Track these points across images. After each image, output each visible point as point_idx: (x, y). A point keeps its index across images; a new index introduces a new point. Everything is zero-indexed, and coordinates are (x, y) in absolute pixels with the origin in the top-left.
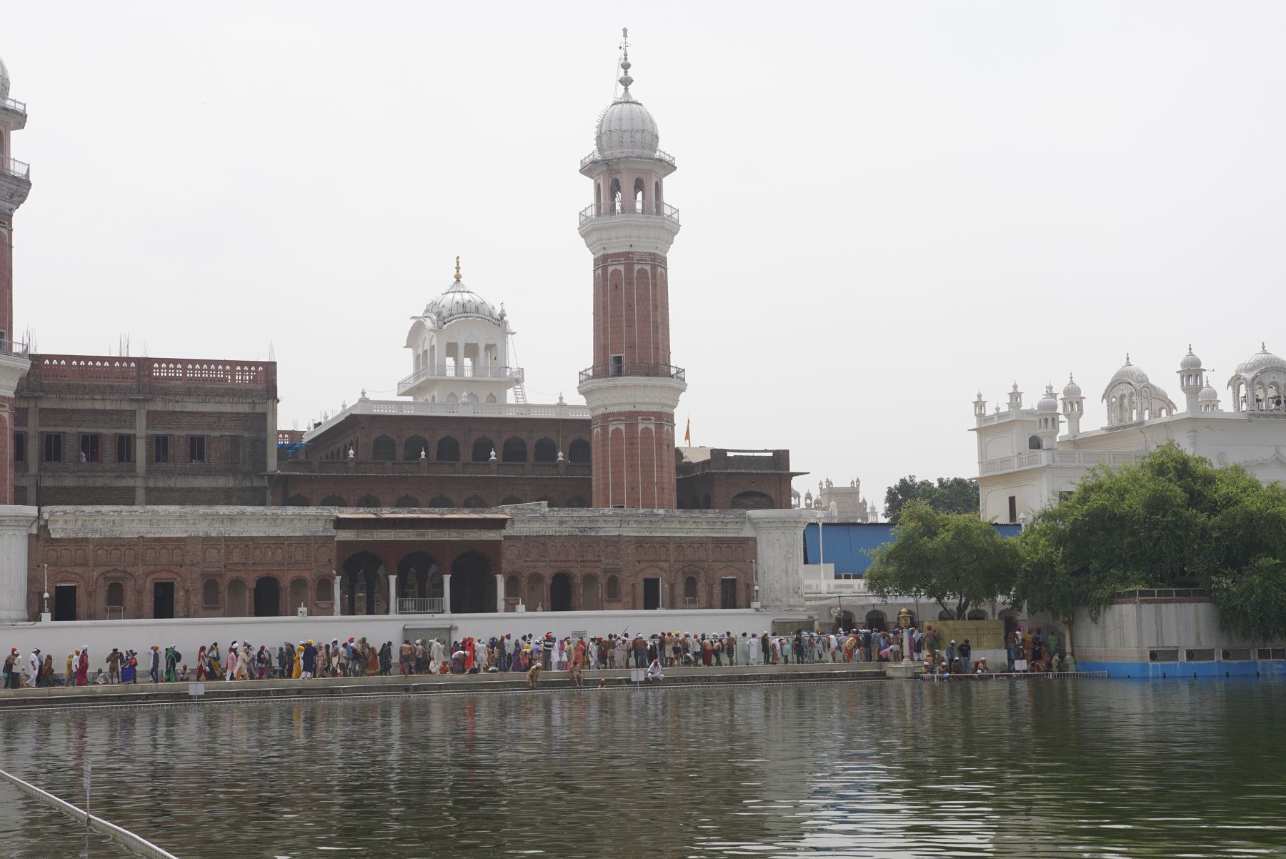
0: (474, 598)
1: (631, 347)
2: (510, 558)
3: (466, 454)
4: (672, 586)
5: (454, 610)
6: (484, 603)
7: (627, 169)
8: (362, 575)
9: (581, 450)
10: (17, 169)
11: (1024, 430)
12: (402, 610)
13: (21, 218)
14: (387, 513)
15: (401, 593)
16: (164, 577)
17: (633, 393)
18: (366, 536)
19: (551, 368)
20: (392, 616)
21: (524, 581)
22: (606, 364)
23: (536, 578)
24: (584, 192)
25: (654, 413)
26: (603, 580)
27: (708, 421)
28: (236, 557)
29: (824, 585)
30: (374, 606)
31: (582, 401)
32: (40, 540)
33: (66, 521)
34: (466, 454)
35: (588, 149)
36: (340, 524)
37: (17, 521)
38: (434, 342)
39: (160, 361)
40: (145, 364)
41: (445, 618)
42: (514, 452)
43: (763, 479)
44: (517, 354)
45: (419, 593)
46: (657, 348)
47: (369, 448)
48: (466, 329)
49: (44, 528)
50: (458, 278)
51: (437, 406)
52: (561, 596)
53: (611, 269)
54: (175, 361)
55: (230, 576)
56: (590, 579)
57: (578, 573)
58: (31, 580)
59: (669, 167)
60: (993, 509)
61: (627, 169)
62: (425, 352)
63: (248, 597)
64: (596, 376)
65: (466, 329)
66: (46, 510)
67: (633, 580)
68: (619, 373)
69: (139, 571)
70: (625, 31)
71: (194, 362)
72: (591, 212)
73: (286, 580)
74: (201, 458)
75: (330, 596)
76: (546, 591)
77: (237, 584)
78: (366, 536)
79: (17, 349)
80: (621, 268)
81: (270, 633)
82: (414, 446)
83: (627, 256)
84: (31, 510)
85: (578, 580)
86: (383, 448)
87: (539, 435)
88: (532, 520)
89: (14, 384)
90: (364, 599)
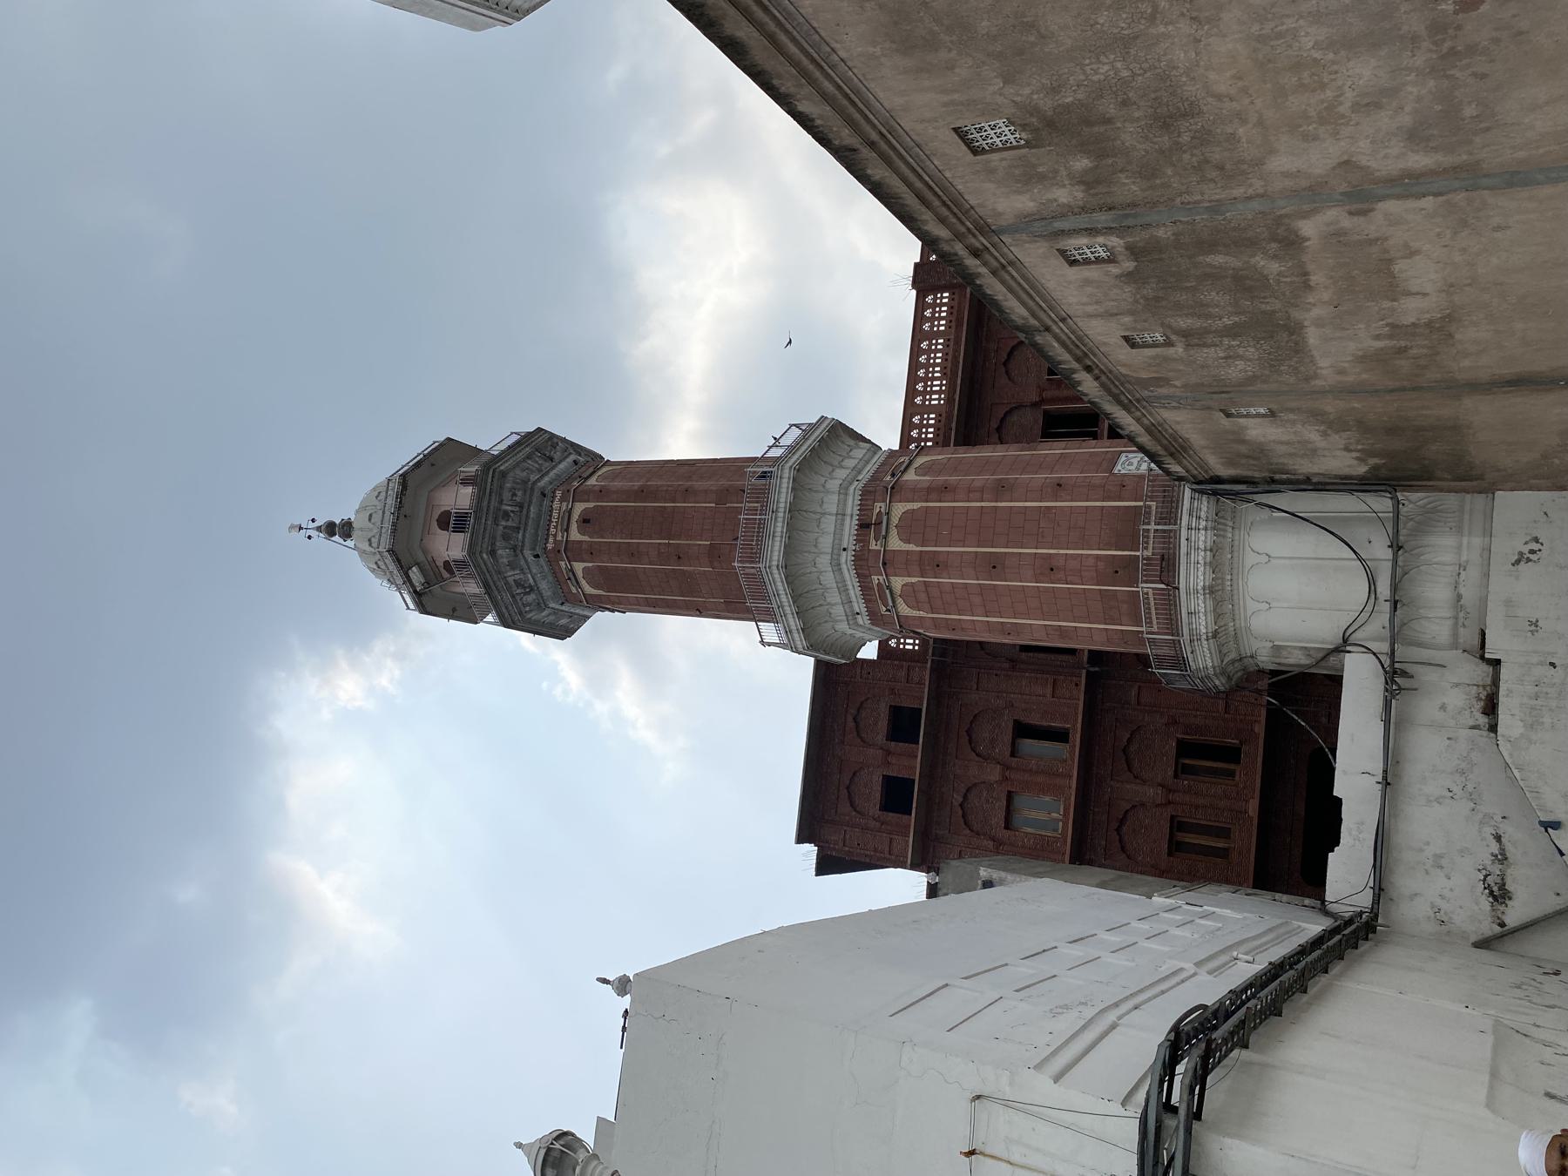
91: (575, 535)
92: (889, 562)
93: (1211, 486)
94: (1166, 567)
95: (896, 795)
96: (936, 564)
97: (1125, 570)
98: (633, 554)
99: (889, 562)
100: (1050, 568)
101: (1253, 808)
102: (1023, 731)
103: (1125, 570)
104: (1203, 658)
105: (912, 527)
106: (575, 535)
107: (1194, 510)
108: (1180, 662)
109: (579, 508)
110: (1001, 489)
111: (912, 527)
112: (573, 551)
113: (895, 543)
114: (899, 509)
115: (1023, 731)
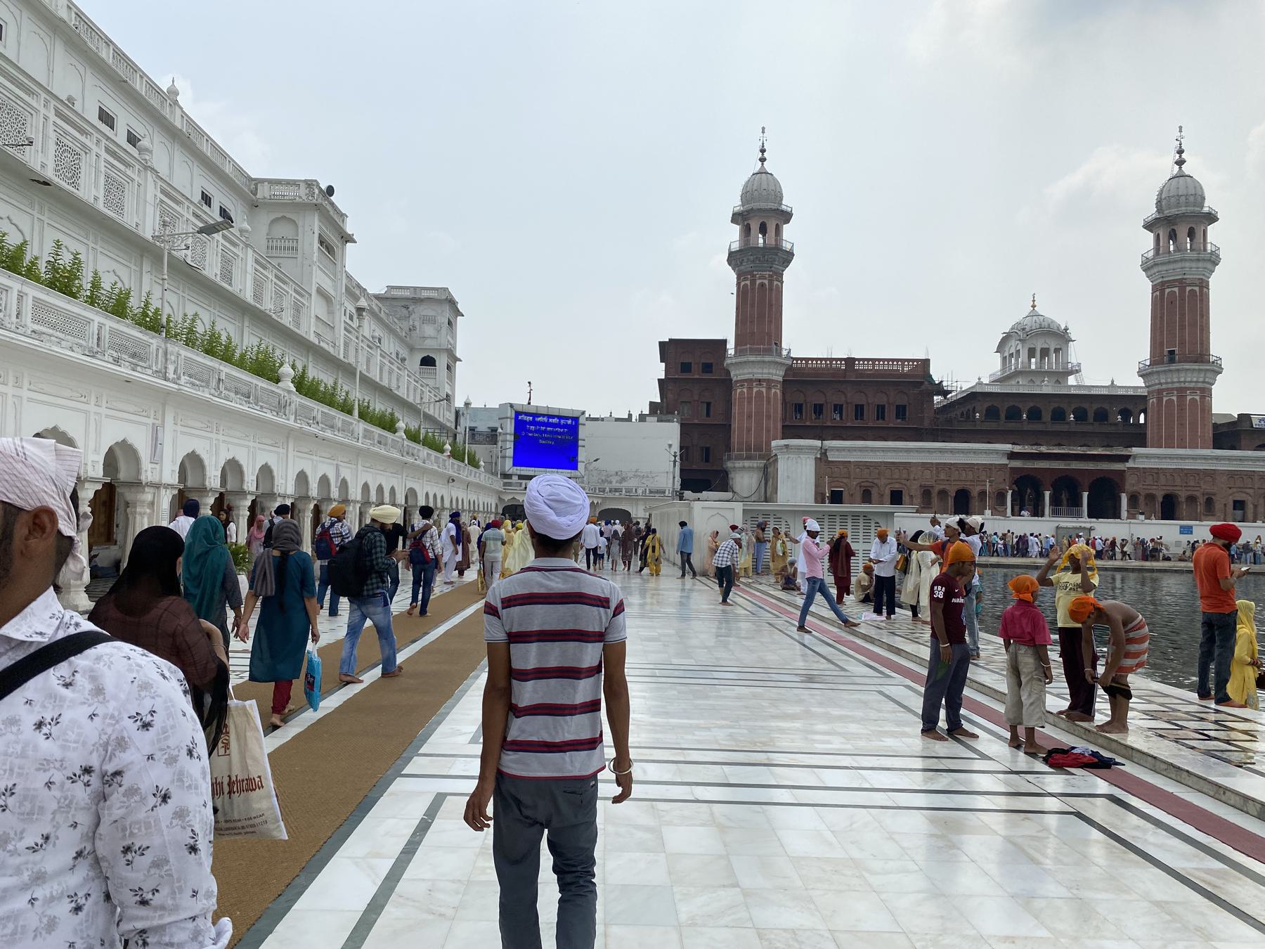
0: (1104, 507)
1: (1182, 343)
2: (1131, 483)
3: (1047, 416)
4: (1256, 506)
5: (1090, 516)
6: (1113, 513)
7: (1180, 220)
8: (1026, 493)
10: (786, 246)
12: (1055, 513)
13: (788, 275)
14: (1044, 449)
15: (1055, 502)
16: (897, 487)
17: (1186, 375)
18: (1030, 465)
20: (1046, 518)
21: (1142, 499)
22: (1161, 355)
23: (1150, 497)
25: (1199, 389)
26: (1202, 500)
28: (942, 476)
30: (1037, 512)
31: (1140, 382)
32: (822, 460)
33: (844, 450)
34: (1047, 416)
35: (1151, 211)
36: (1012, 456)
37: (811, 448)
38: (1020, 347)
39: (859, 360)
40: (850, 361)
41: (1085, 522)
44: (1075, 354)
46: (1202, 344)
47: (983, 413)
49: (824, 453)
50: (1034, 306)
51: (1021, 387)
52: (1169, 510)
53: (1167, 291)
54: (868, 360)
55: (938, 488)
56: (1192, 499)
57: (1183, 495)
58: (816, 486)
59: (1212, 218)
61: (1180, 220)
62: (1011, 355)
63: (951, 502)
64: (1153, 363)
65: (1041, 340)
66: (828, 443)
68: (1172, 361)
69: (882, 482)
70: (1181, 128)
71: (879, 360)
72: (1151, 254)
73: (975, 492)
74: (883, 418)
75: (1004, 503)
76: (1158, 507)
77: (943, 494)
78: (1030, 465)
79: (784, 353)
80: (1176, 289)
82: (1013, 414)
83: (1180, 281)
84: (818, 443)
85: (1182, 499)
86: (992, 413)
87: (1095, 406)
89: (782, 373)
91: (758, 282)
92: (750, 389)
93: (766, 467)
94: (749, 458)
95: (686, 368)
96: (750, 402)
97: (749, 449)
98: (752, 305)
99: (750, 389)
100: (749, 430)
101: (694, 467)
102: (709, 404)
103: (749, 449)
104: (729, 464)
105: (759, 393)
106: (758, 282)
107: (761, 463)
108: (729, 459)
109: (766, 282)
110: (768, 417)
111: (759, 393)
112: (753, 282)
113: (755, 390)
114: (764, 390)
115: (709, 404)
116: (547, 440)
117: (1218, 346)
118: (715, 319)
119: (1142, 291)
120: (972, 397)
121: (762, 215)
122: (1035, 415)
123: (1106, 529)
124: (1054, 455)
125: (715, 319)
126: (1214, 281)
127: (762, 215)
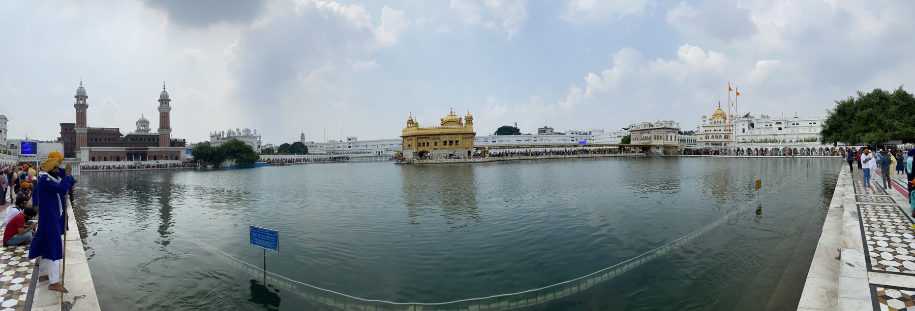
0: (144, 159)
7: (164, 100)
9: (158, 139)
11: (218, 137)
17: (165, 131)
19: (154, 128)
24: (158, 104)
27: (175, 135)
29: (190, 157)
35: (159, 98)
42: (149, 139)
43: (182, 143)
45: (137, 157)
48: (143, 123)
52: (155, 159)
60: (213, 146)
61: (164, 100)
67: (164, 156)
81: (117, 164)
86: (132, 139)
88: (151, 149)
90: (130, 159)
116: (29, 147)
117: (171, 126)
118: (72, 119)
119: (158, 114)
120: (128, 136)
121: (81, 96)
122: (141, 139)
123: (143, 163)
124: (134, 148)
125: (72, 119)
126: (171, 113)
127: (81, 96)
